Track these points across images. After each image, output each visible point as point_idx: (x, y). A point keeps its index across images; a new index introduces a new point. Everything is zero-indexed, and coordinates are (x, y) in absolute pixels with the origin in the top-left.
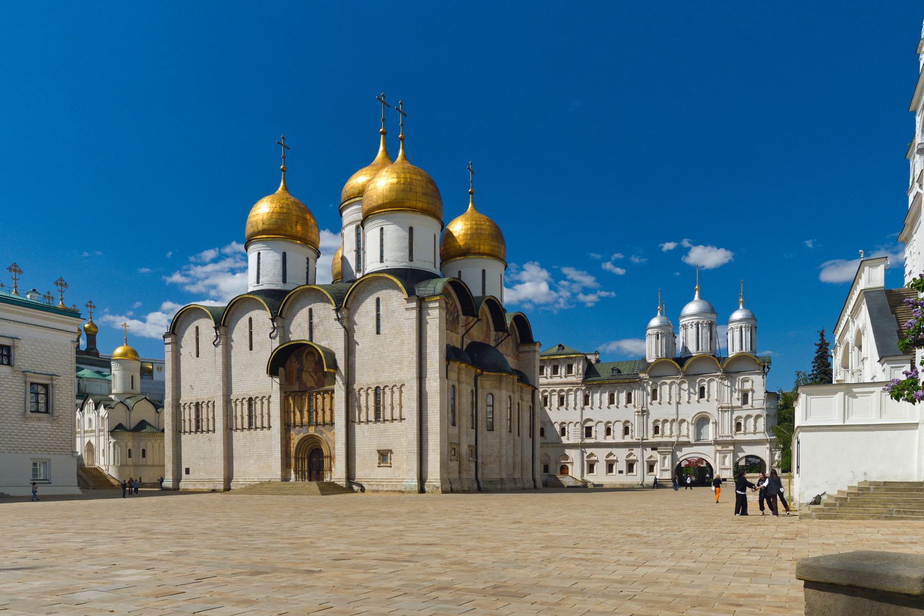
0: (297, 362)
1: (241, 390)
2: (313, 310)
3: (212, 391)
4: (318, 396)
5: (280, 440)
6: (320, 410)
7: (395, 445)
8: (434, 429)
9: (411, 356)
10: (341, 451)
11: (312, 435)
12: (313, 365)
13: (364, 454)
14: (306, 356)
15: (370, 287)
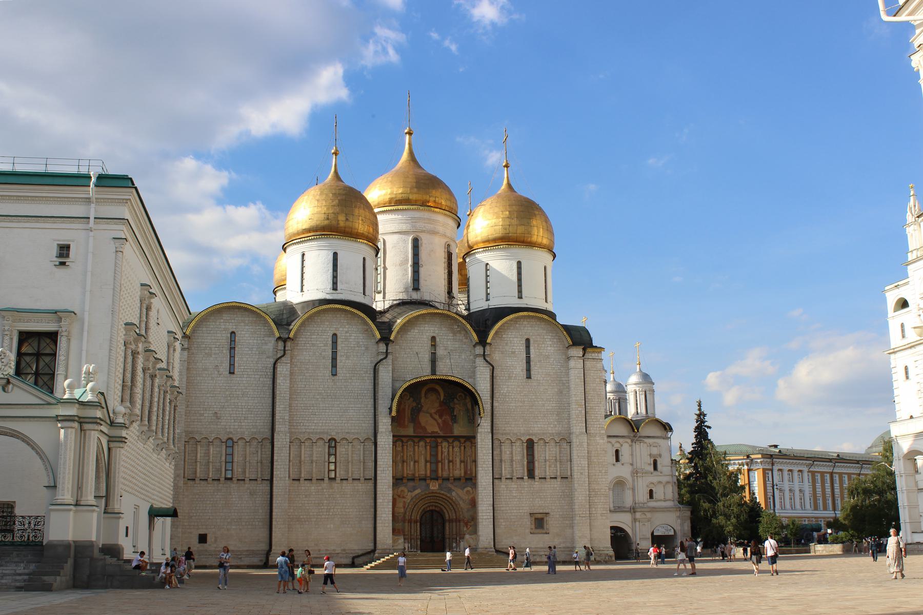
0: (411, 399)
1: (313, 427)
2: (438, 340)
3: (257, 424)
4: (445, 444)
5: (391, 498)
6: (446, 461)
7: (554, 508)
8: (602, 490)
9: (579, 409)
10: (488, 514)
11: (436, 493)
12: (437, 405)
13: (513, 517)
14: (425, 395)
15: (517, 325)
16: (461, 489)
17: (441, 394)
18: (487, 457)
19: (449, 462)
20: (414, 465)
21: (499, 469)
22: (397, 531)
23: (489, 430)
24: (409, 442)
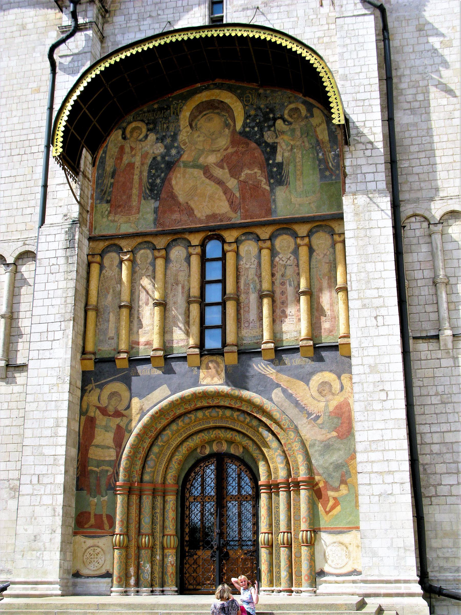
5: (64, 414)
6: (253, 297)
16: (302, 379)
17: (236, 114)
18: (380, 266)
19: (261, 297)
20: (152, 315)
21: (429, 308)
22: (92, 521)
23: (383, 185)
24: (142, 251)
